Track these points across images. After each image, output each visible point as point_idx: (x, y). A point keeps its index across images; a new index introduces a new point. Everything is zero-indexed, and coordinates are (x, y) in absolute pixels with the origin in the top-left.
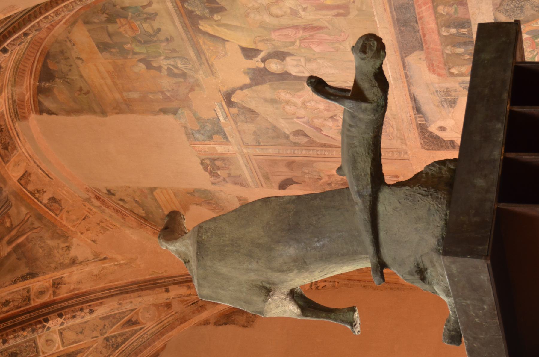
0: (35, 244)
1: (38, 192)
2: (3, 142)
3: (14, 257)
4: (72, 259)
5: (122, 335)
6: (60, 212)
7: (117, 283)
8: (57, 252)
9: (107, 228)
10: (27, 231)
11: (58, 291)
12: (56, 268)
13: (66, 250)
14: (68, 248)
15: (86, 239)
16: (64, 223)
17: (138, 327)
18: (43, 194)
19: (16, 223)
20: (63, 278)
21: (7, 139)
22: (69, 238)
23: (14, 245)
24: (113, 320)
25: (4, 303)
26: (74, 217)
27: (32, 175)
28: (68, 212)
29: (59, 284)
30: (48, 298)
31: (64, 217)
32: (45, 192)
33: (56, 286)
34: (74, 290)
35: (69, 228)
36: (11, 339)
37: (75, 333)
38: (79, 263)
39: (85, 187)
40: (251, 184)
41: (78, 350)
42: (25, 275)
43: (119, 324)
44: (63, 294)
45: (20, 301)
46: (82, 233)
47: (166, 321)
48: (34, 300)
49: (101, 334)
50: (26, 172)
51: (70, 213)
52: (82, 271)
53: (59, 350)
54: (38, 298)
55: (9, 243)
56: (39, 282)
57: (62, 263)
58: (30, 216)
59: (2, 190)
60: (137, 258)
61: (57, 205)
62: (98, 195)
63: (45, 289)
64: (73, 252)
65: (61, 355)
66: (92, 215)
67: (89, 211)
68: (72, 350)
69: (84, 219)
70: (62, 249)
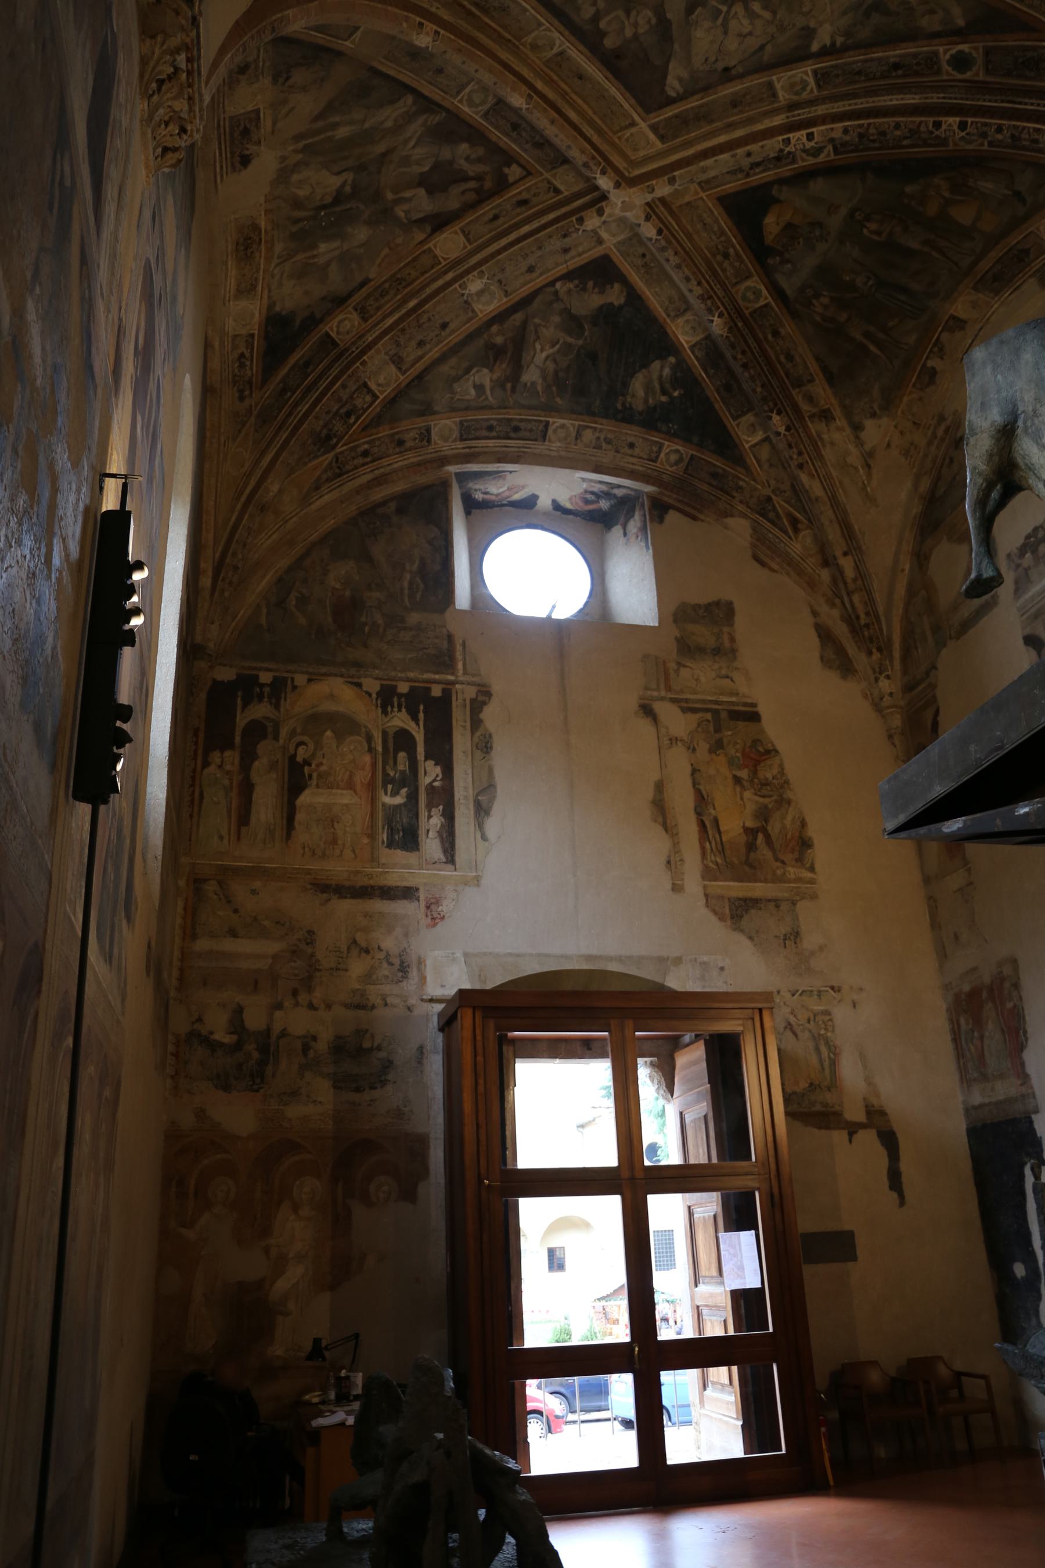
1: (941, 350)
5: (778, 516)
7: (840, 491)
14: (873, 415)
16: (905, 399)
17: (790, 531)
24: (793, 501)
28: (920, 399)
29: (825, 417)
32: (942, 358)
34: (821, 439)
40: (1021, 601)
43: (790, 509)
46: (896, 427)
47: (805, 565)
49: (773, 491)
64: (869, 423)
69: (914, 423)
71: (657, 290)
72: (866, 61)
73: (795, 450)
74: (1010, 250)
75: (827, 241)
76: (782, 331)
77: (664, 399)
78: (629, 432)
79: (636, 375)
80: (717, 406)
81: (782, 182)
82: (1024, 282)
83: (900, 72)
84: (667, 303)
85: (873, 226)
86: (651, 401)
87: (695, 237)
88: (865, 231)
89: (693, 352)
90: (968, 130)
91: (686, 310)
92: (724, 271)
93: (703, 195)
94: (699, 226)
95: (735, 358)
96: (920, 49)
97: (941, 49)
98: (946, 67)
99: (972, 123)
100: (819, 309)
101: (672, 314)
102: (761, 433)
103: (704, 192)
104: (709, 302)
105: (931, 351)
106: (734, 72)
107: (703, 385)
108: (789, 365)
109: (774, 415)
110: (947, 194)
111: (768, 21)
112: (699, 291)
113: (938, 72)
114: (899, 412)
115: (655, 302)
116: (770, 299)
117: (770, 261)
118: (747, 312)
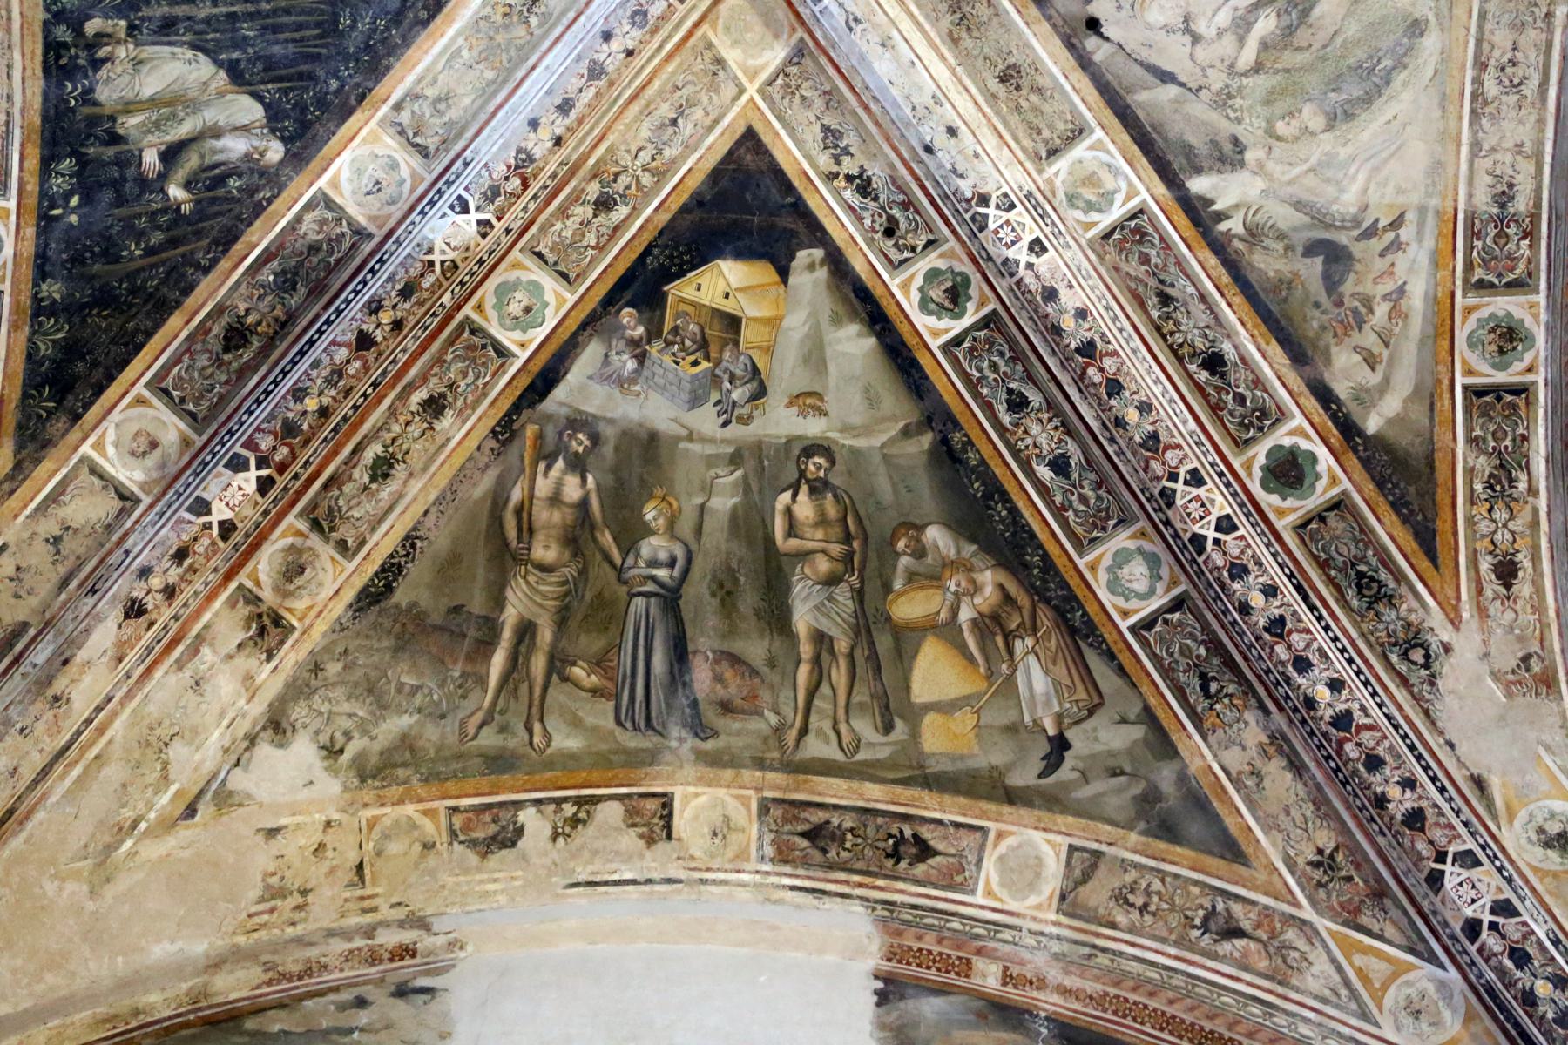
0: (442, 685)
1: (575, 822)
2: (849, 836)
3: (477, 604)
4: (289, 730)
6: (451, 825)
7: (76, 772)
8: (355, 715)
9: (268, 905)
10: (501, 702)
11: (243, 610)
12: (317, 668)
13: (332, 738)
14: (332, 752)
15: (299, 819)
16: (410, 809)
18: (555, 828)
19: (557, 694)
20: (264, 656)
21: (844, 854)
22: (356, 781)
23: (507, 634)
25: (391, 466)
26: (394, 848)
27: (642, 843)
28: (428, 846)
29: (262, 631)
30: (255, 568)
31: (428, 825)
32: (555, 837)
34: (195, 650)
35: (382, 805)
36: (348, 362)
37: (74, 525)
38: (257, 734)
39: (469, 948)
41: (25, 479)
44: (216, 615)
45: (341, 502)
46: (328, 824)
48: (299, 534)
50: (669, 837)
51: (417, 848)
52: (225, 722)
53: (91, 441)
54: (292, 549)
55: (526, 631)
57: (309, 697)
58: (531, 744)
59: (696, 735)
60: (92, 893)
61: (480, 834)
62: (408, 962)
63: (292, 587)
64: (303, 750)
65: (72, 426)
66: (346, 900)
67: (366, 904)
68: (46, 466)
69: (360, 867)
70: (348, 736)
71: (465, 53)
72: (1203, 298)
73: (174, 574)
74: (906, 818)
75: (725, 424)
76: (447, 422)
77: (151, 159)
78: (17, 74)
79: (201, 57)
80: (175, 321)
81: (837, 262)
82: (843, 896)
83: (1203, 376)
84: (431, 92)
85: (805, 508)
86: (134, 120)
87: (635, 108)
88: (786, 497)
89: (309, 206)
90: (1228, 538)
91: (423, 151)
92: (563, 213)
93: (752, 90)
94: (666, 110)
95: (375, 307)
96: (1277, 384)
97: (1298, 420)
98: (1260, 453)
99: (1242, 538)
100: (543, 487)
101: (405, 117)
102: (139, 476)
103: (760, 91)
104: (516, 182)
105: (559, 802)
106: (1091, 42)
107: (224, 264)
108: (361, 475)
109: (253, 473)
110: (965, 614)
111: (1232, 66)
112: (539, 144)
113: (1241, 444)
115: (428, 59)
116: (524, 355)
117: (627, 316)
118: (468, 310)
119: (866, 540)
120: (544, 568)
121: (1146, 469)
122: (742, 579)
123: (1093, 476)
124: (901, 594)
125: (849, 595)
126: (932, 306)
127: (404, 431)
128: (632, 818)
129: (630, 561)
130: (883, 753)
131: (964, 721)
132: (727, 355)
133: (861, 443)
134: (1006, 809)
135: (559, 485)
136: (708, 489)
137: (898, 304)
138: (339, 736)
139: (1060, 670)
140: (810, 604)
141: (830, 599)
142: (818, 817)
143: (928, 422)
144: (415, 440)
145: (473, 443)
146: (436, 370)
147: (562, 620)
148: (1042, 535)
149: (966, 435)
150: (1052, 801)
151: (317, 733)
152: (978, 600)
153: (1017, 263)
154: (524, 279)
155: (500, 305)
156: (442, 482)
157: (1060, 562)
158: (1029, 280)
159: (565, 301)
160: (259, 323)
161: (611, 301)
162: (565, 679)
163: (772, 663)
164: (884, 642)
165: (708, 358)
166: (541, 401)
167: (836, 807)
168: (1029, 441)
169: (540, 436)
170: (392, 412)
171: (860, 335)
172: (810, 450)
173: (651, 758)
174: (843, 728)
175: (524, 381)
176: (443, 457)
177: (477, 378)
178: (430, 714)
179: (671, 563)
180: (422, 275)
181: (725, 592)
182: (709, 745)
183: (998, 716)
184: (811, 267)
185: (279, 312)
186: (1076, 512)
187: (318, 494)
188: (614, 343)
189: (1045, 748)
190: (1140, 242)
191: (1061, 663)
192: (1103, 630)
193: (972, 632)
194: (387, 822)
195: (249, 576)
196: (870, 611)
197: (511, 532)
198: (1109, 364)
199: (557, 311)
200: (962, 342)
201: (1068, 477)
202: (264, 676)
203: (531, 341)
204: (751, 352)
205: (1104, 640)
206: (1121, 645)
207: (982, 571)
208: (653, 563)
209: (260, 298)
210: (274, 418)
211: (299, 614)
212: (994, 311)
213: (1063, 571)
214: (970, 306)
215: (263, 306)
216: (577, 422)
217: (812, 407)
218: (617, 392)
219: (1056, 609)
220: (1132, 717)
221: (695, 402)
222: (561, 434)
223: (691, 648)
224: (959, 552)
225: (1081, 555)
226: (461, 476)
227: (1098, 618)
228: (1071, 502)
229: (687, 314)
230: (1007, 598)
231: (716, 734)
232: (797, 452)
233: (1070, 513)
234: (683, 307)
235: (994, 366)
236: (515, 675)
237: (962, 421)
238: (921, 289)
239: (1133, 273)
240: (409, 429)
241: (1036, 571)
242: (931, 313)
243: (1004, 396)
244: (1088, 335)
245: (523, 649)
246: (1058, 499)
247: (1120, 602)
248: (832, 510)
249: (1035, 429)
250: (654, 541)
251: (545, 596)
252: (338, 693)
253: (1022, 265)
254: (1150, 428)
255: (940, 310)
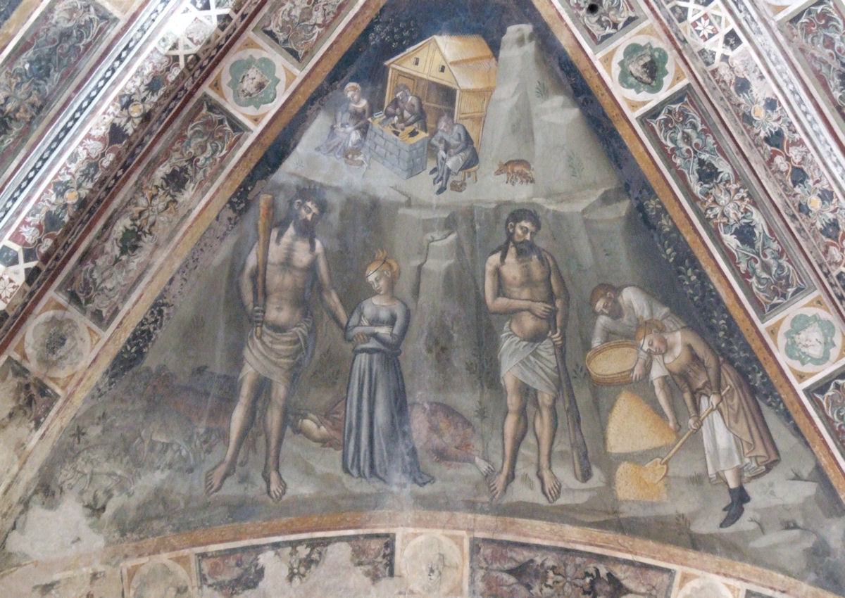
0: (189, 440)
1: (309, 562)
2: (551, 574)
3: (218, 364)
4: (58, 491)
6: (201, 570)
8: (115, 474)
12: (79, 433)
13: (95, 497)
14: (95, 509)
15: (69, 573)
16: (164, 557)
18: (291, 569)
19: (291, 446)
20: (32, 425)
21: (547, 591)
22: (117, 535)
23: (245, 391)
25: (139, 238)
27: (367, 580)
28: (181, 590)
29: (30, 401)
31: (180, 571)
33: (33, 391)
35: (140, 556)
38: (30, 497)
42: (146, 345)
45: (95, 275)
46: (94, 576)
48: (59, 306)
50: (391, 574)
51: (172, 592)
54: (53, 321)
55: (262, 387)
56: (90, 361)
58: (269, 492)
59: (415, 481)
61: (226, 577)
63: (54, 358)
64: (71, 511)
70: (109, 494)
75: (441, 191)
76: (188, 194)
85: (512, 269)
88: (495, 259)
100: (276, 252)
105: (294, 544)
108: (112, 248)
110: (657, 372)
114: (130, 563)
116: (257, 130)
118: (206, 88)
119: (567, 302)
120: (278, 328)
121: (826, 252)
122: (456, 336)
123: (775, 246)
124: (599, 352)
125: (551, 351)
126: (632, 80)
127: (150, 205)
128: (359, 556)
129: (354, 320)
130: (582, 499)
131: (653, 472)
132: (442, 125)
133: (565, 208)
134: (692, 554)
135: (290, 250)
136: (424, 251)
137: (600, 77)
138: (102, 497)
139: (742, 427)
140: (515, 361)
141: (535, 354)
142: (525, 555)
143: (625, 189)
144: (160, 213)
145: (213, 213)
146: (177, 146)
147: (294, 375)
148: (727, 300)
149: (660, 203)
150: (733, 549)
151: (82, 493)
152: (668, 359)
153: (713, 54)
154: (257, 57)
155: (234, 84)
156: (185, 251)
157: (744, 326)
158: (724, 72)
159: (295, 77)
160: (17, 110)
161: (336, 77)
162: (298, 431)
163: (482, 414)
164: (583, 397)
165: (425, 129)
166: (273, 172)
167: (539, 547)
168: (718, 210)
169: (272, 206)
170: (139, 187)
171: (564, 106)
172: (519, 214)
173: (374, 502)
174: (546, 475)
175: (258, 154)
176: (185, 227)
177: (214, 152)
178: (180, 469)
179: (392, 321)
180: (168, 69)
181: (441, 348)
182: (427, 489)
183: (684, 468)
184: (521, 41)
185: (34, 98)
186: (759, 279)
187: (74, 269)
188: (340, 114)
189: (726, 500)
190: (825, 26)
191: (742, 419)
192: (781, 391)
193: (663, 388)
194: (144, 570)
195: (16, 350)
196: (570, 368)
197: (248, 297)
198: (795, 153)
199: (287, 87)
200: (659, 114)
201: (752, 245)
202: (33, 443)
203: (264, 115)
204: (461, 122)
205: (782, 401)
206: (797, 406)
207: (672, 332)
208: (375, 322)
209: (18, 86)
210: (39, 211)
211: (61, 383)
212: (689, 86)
213: (746, 335)
214: (667, 80)
215: (21, 93)
216: (307, 191)
217: (520, 174)
218: (342, 162)
219: (739, 369)
220: (805, 475)
221: (413, 170)
222: (291, 203)
223: (410, 400)
224: (652, 314)
225: (763, 319)
226: (201, 246)
227: (777, 381)
228: (754, 270)
229: (406, 87)
230: (695, 358)
231: (432, 480)
232: (505, 216)
233: (754, 280)
234: (402, 81)
235: (687, 138)
236: (254, 429)
237: (657, 189)
238: (621, 64)
239: (817, 55)
240: (155, 202)
241: (721, 334)
242: (630, 86)
243: (696, 167)
244: (776, 125)
245: (259, 405)
246: (743, 267)
247: (797, 365)
248: (537, 272)
249: (723, 199)
250: (376, 301)
251: (279, 355)
252: (99, 454)
253: (718, 57)
254: (831, 216)
255: (639, 84)
